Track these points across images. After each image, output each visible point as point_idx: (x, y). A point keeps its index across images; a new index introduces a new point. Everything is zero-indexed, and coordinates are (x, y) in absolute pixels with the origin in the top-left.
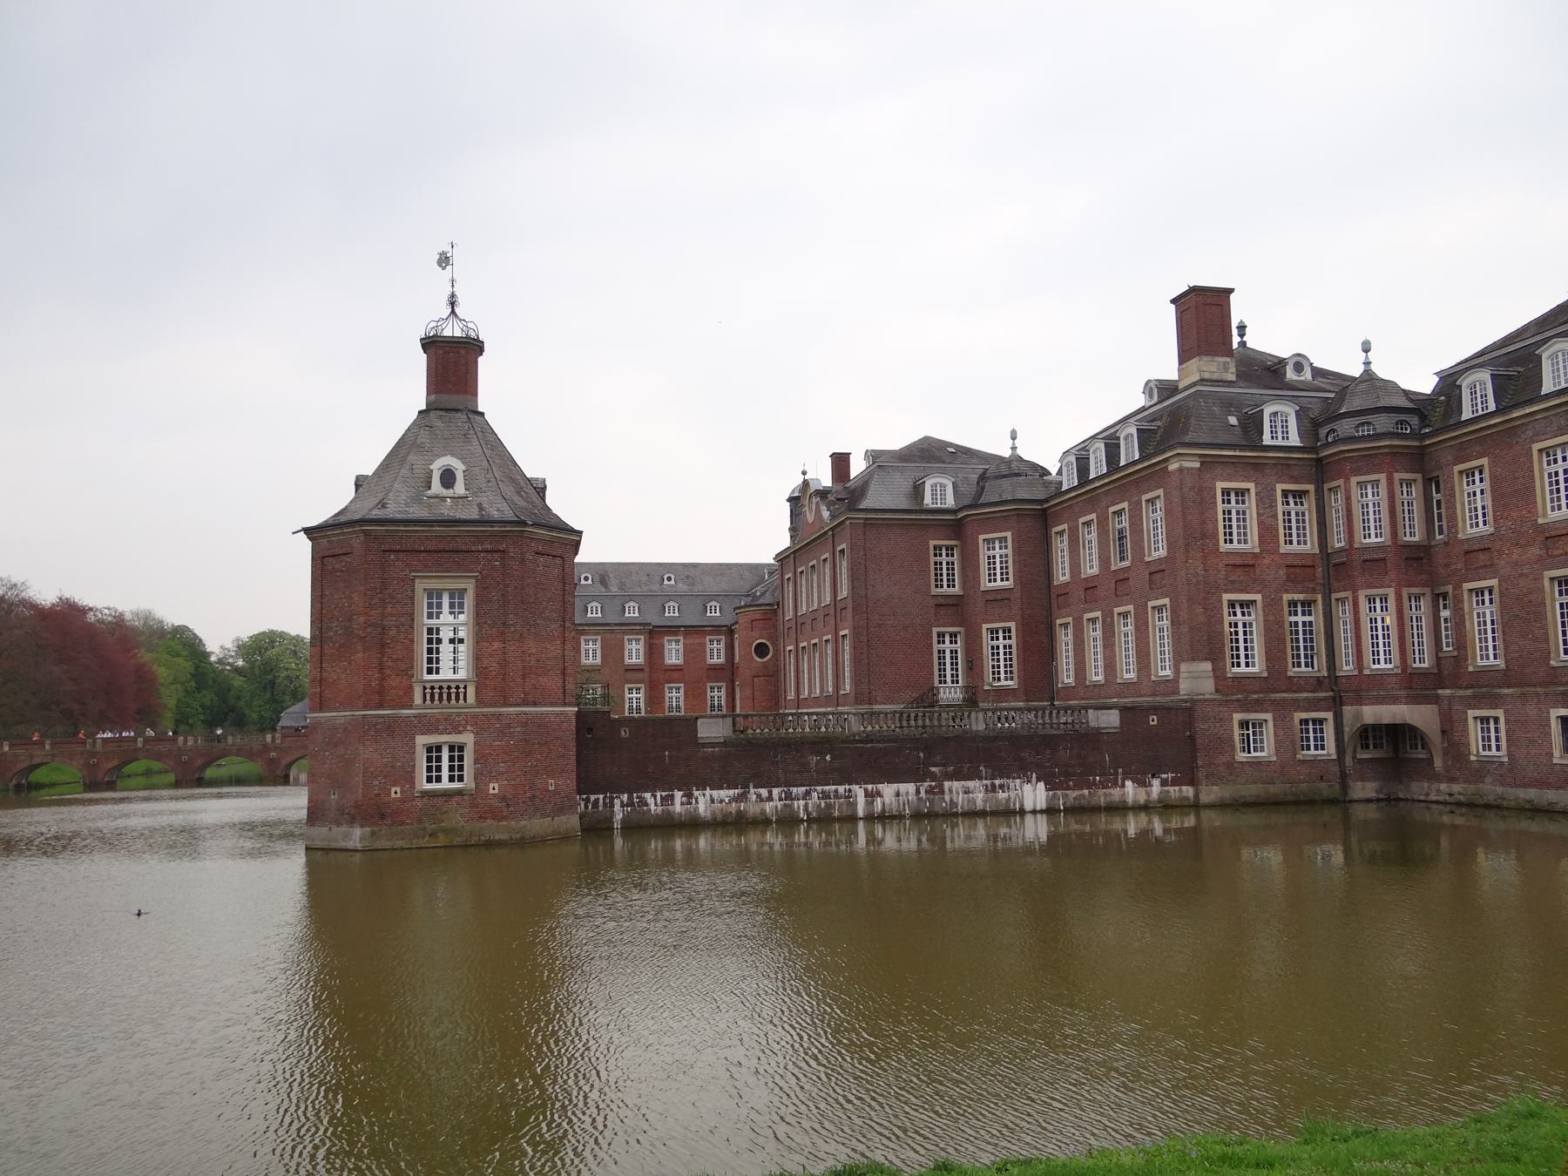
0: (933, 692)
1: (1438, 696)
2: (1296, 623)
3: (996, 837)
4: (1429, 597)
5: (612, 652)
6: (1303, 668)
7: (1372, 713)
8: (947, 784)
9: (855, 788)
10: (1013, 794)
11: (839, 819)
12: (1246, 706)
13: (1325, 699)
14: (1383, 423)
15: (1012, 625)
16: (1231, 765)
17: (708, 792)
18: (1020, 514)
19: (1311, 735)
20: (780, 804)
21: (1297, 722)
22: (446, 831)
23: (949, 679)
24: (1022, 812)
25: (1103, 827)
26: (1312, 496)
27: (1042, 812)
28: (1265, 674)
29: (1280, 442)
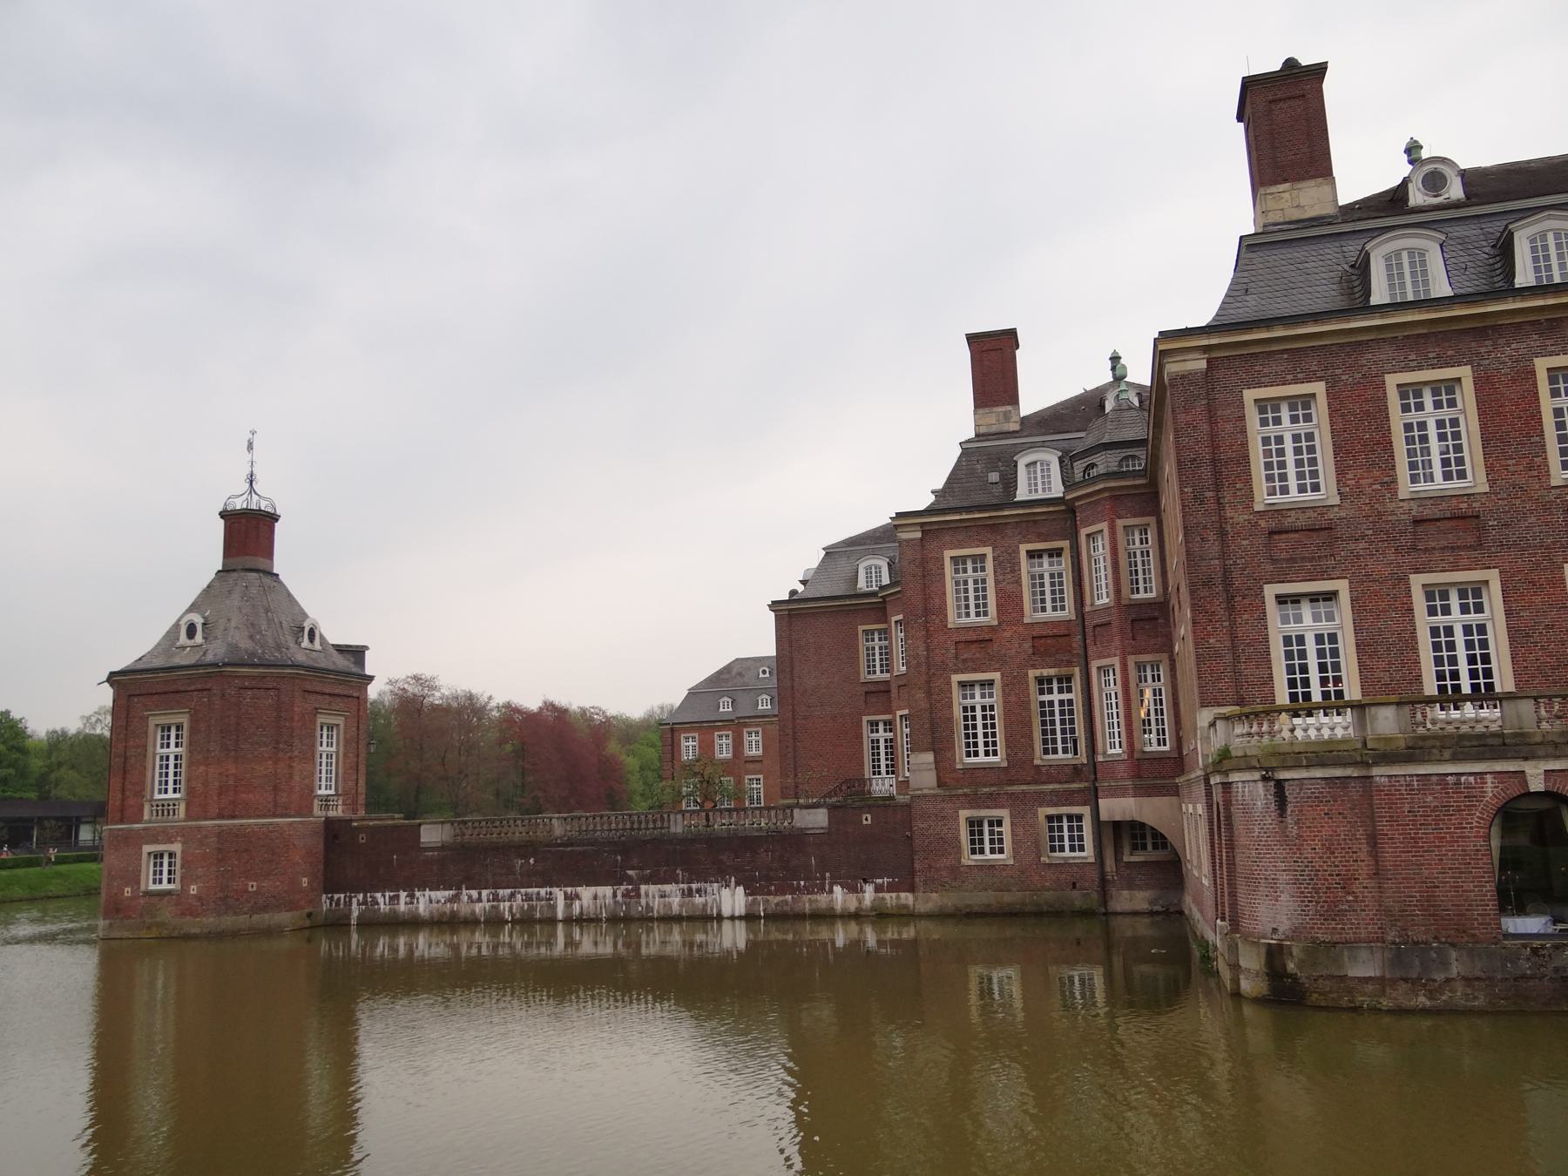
0: (863, 781)
2: (1051, 703)
3: (691, 945)
6: (1060, 755)
8: (643, 888)
9: (556, 890)
10: (710, 899)
11: (540, 921)
12: (975, 801)
13: (1080, 791)
16: (956, 870)
17: (427, 892)
19: (1066, 834)
20: (488, 905)
21: (1041, 818)
22: (158, 925)
24: (720, 918)
25: (807, 936)
26: (1067, 555)
27: (740, 918)
28: (1005, 764)
29: (1040, 495)
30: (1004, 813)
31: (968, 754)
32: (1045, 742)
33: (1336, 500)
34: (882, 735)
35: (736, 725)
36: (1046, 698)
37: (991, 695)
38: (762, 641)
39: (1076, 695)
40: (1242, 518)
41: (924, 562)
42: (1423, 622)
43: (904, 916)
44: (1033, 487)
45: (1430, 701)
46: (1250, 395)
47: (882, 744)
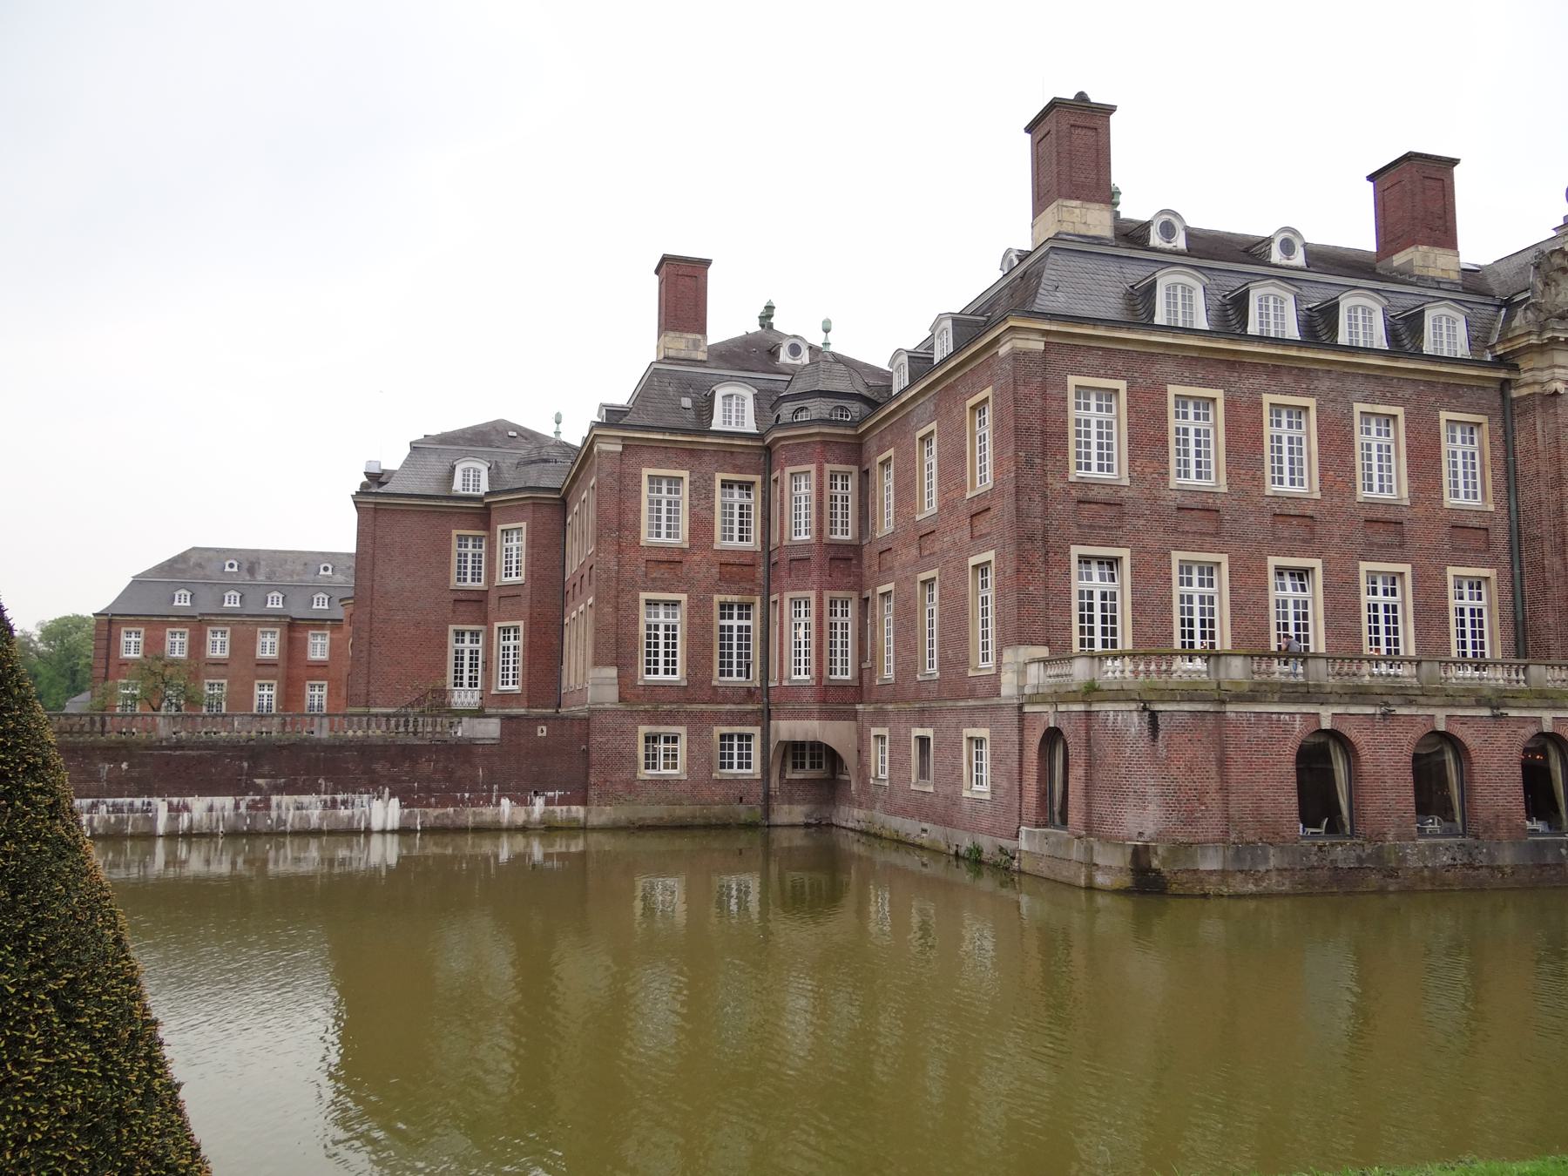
0: (443, 692)
1: (856, 712)
2: (730, 628)
3: (331, 862)
4: (856, 599)
5: (243, 645)
6: (735, 678)
7: (788, 729)
8: (275, 799)
10: (357, 811)
11: (132, 837)
12: (654, 718)
13: (753, 712)
14: (818, 408)
15: (521, 624)
16: (632, 785)
18: (537, 504)
19: (736, 752)
21: (716, 737)
23: (466, 681)
24: (368, 832)
25: (468, 850)
26: (758, 487)
27: (393, 832)
28: (685, 683)
29: (733, 428)
30: (681, 730)
31: (648, 671)
32: (722, 664)
33: (1126, 482)
34: (467, 645)
35: (198, 625)
36: (726, 622)
37: (674, 616)
38: (335, 531)
39: (754, 622)
40: (1058, 486)
41: (621, 477)
42: (1177, 590)
43: (582, 829)
44: (727, 419)
45: (1270, 656)
46: (1073, 381)
47: (467, 656)
